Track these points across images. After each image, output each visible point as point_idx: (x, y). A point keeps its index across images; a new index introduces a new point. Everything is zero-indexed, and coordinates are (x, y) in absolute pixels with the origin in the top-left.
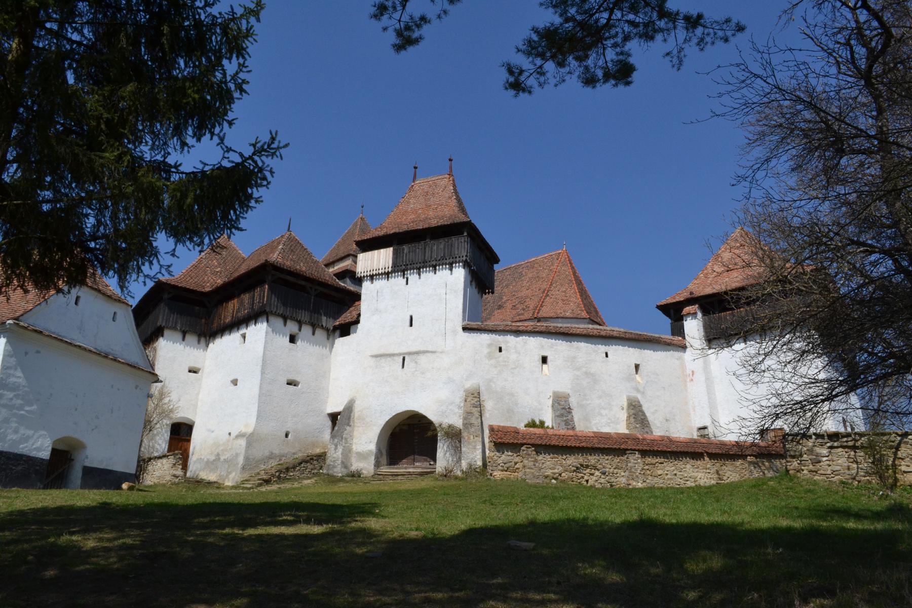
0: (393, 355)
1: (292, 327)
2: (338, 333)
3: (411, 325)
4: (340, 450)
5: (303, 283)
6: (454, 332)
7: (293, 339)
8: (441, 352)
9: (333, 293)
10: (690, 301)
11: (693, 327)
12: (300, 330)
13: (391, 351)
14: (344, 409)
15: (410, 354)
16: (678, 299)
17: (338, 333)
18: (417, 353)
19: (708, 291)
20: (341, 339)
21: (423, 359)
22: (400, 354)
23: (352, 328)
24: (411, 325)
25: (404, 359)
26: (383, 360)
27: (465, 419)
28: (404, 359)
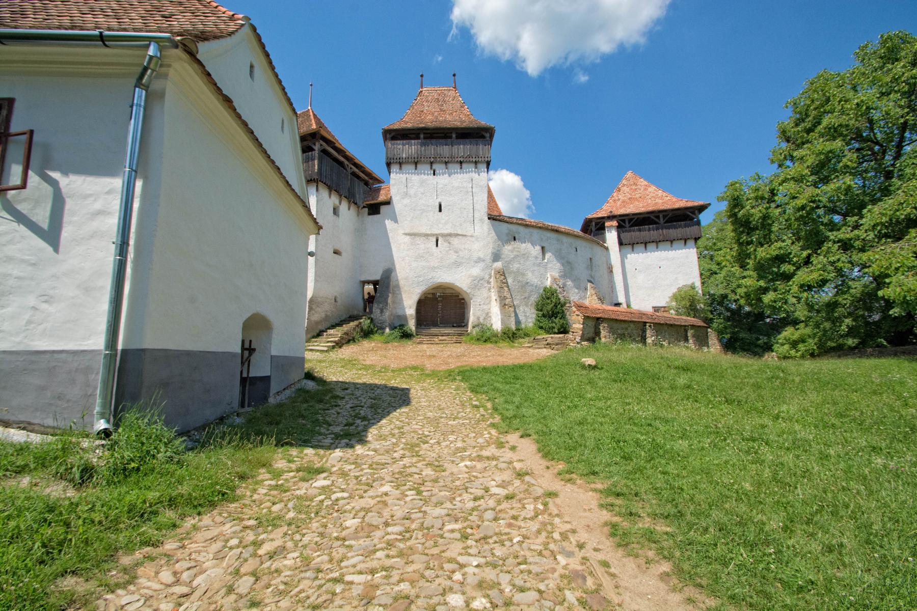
0: (427, 235)
1: (335, 199)
2: (366, 210)
3: (440, 210)
4: (387, 314)
5: (342, 159)
6: (481, 220)
7: (336, 211)
8: (472, 236)
9: (362, 175)
10: (611, 217)
11: (611, 237)
12: (340, 203)
13: (424, 230)
14: (382, 278)
15: (443, 235)
16: (600, 215)
17: (366, 210)
18: (450, 235)
19: (622, 211)
20: (371, 217)
21: (455, 241)
22: (432, 235)
23: (383, 209)
24: (440, 210)
25: (437, 241)
26: (417, 238)
27: (499, 292)
28: (437, 241)
